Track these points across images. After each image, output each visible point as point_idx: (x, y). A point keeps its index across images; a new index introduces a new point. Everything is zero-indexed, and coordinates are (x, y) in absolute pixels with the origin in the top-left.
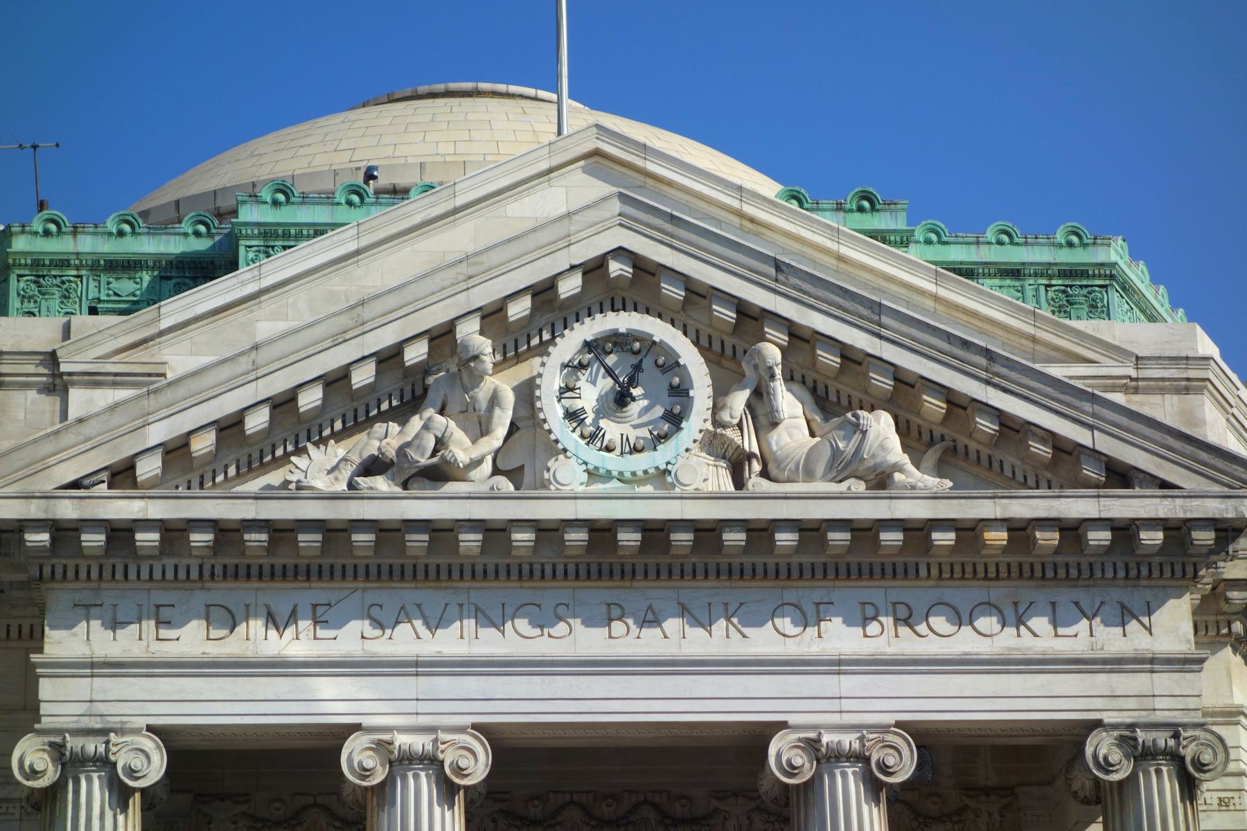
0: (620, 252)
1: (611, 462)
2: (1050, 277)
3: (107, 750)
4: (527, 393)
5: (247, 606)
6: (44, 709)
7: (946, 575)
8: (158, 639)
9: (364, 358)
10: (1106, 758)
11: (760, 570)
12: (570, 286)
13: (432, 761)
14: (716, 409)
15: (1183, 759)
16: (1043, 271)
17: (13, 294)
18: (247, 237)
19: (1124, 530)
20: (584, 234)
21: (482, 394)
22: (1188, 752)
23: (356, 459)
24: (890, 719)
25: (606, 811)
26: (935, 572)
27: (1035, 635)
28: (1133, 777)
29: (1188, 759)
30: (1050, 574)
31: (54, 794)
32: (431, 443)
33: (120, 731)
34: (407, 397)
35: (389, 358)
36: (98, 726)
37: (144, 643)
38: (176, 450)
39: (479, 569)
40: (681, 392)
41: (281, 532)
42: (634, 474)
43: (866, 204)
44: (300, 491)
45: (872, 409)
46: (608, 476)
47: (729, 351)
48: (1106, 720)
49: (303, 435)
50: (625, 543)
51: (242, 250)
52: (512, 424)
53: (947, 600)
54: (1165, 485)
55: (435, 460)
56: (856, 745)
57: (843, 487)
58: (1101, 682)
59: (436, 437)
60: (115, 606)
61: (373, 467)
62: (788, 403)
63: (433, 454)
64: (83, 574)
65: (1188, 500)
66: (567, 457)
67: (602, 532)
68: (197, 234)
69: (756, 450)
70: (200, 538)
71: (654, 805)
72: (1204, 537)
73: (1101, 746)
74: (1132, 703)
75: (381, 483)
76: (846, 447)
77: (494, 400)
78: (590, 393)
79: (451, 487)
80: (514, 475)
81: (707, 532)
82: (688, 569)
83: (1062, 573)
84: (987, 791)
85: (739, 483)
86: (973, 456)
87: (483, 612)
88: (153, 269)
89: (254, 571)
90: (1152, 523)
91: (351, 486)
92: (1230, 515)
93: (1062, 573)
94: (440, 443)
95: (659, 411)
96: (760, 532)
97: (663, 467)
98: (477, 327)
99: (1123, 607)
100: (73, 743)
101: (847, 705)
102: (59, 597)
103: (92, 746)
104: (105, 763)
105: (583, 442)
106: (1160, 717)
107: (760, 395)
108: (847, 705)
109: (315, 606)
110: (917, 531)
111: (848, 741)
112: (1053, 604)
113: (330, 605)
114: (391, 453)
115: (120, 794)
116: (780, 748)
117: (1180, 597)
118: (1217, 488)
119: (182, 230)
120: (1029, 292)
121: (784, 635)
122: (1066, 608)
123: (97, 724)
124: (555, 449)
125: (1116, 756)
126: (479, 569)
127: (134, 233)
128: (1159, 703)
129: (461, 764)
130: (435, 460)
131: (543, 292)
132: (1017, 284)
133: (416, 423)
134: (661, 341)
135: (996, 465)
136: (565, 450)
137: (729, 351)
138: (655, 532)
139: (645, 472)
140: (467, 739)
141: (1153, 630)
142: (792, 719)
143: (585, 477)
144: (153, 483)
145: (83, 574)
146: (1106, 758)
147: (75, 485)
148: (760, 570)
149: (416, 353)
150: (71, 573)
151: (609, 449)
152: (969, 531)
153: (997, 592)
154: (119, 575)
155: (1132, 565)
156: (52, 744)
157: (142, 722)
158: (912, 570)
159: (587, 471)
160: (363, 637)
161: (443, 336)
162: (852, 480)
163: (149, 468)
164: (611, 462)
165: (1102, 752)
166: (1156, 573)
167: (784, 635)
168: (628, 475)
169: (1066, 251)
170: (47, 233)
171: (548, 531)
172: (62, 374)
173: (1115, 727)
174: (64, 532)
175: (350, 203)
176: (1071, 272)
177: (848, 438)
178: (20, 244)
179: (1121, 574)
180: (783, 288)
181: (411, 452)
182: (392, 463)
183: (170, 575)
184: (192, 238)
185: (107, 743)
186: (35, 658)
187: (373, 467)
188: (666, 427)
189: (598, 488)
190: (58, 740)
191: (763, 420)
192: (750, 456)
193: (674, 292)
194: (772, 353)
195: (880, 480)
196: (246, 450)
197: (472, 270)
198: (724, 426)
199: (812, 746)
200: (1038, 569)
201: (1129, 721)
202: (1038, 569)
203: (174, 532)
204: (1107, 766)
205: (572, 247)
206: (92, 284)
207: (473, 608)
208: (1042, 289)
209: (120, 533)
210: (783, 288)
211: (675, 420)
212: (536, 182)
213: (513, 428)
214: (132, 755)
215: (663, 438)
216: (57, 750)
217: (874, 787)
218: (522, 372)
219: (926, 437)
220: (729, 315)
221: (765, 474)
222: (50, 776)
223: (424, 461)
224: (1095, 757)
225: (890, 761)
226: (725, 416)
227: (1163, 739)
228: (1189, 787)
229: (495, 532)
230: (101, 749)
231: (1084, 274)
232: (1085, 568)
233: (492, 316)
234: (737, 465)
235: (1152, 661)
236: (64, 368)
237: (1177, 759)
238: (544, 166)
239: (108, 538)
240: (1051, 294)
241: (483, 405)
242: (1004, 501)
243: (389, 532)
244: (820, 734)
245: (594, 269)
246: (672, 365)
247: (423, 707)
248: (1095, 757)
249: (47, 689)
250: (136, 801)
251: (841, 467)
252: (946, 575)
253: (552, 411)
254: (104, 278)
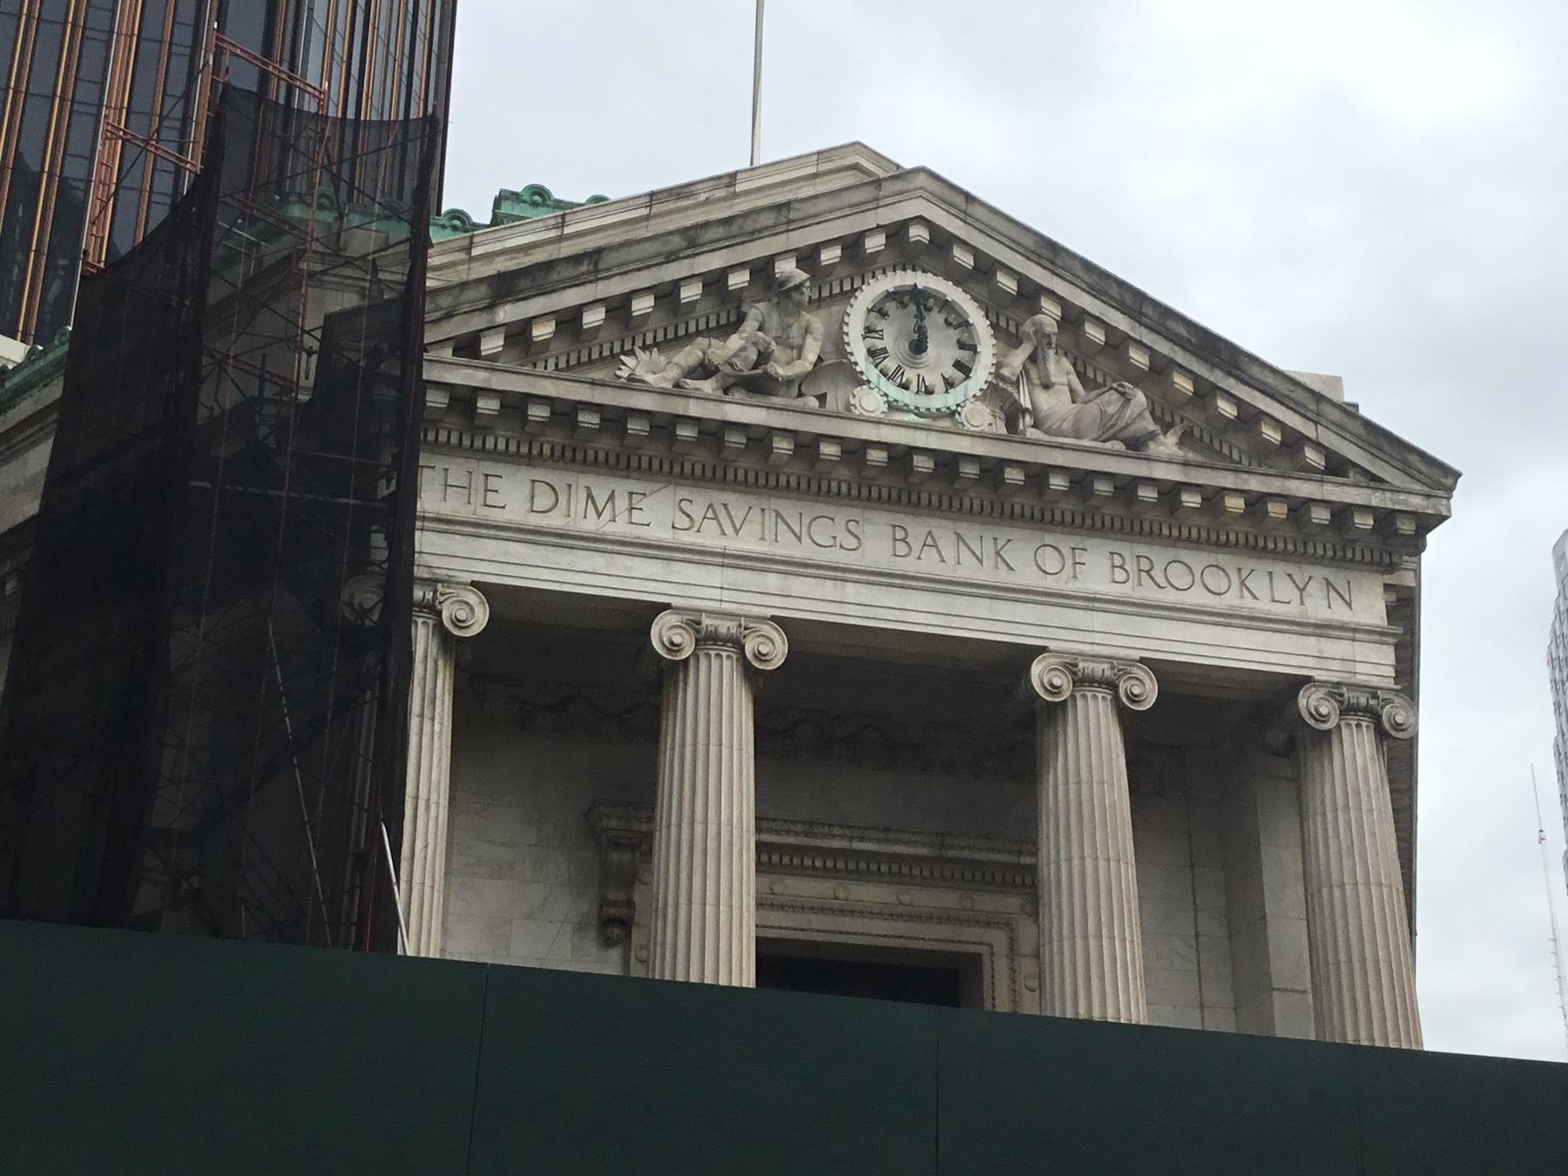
0: (921, 220)
1: (906, 397)
3: (435, 598)
8: (486, 505)
9: (693, 276)
10: (1316, 709)
14: (998, 366)
19: (1342, 513)
20: (890, 200)
24: (1137, 655)
27: (1255, 597)
29: (1384, 718)
32: (754, 356)
33: (447, 582)
35: (715, 282)
36: (426, 576)
37: (472, 507)
38: (518, 334)
42: (928, 409)
44: (633, 383)
46: (905, 409)
48: (1317, 678)
50: (920, 469)
53: (1182, 559)
54: (1375, 478)
55: (759, 371)
56: (1108, 673)
57: (1108, 445)
58: (1311, 644)
59: (759, 351)
60: (446, 470)
62: (1059, 369)
63: (755, 366)
65: (1396, 494)
66: (870, 388)
67: (901, 456)
69: (1029, 406)
73: (1309, 701)
74: (1336, 665)
75: (707, 386)
78: (892, 337)
87: (782, 518)
90: (1365, 509)
91: (677, 385)
92: (1430, 512)
97: (954, 408)
98: (794, 265)
99: (1328, 583)
101: (1098, 638)
105: (883, 379)
106: (1360, 679)
108: (1098, 638)
110: (1170, 492)
112: (1270, 573)
113: (644, 494)
116: (1038, 671)
118: (1418, 487)
119: (441, 222)
121: (1045, 572)
124: (858, 380)
128: (1360, 668)
129: (763, 651)
130: (759, 371)
131: (852, 245)
133: (735, 342)
134: (953, 301)
136: (869, 382)
139: (938, 410)
140: (767, 629)
141: (1353, 605)
142: (1052, 645)
143: (885, 408)
144: (493, 358)
146: (1316, 709)
151: (905, 387)
152: (1213, 497)
157: (468, 578)
159: (888, 402)
160: (674, 527)
162: (1114, 442)
163: (492, 344)
164: (906, 397)
165: (1313, 703)
167: (1045, 572)
168: (923, 410)
172: (380, 281)
173: (1323, 683)
184: (449, 231)
185: (435, 592)
187: (704, 370)
195: (1136, 445)
199: (1071, 668)
201: (1336, 680)
205: (879, 210)
207: (773, 514)
212: (802, 184)
214: (457, 606)
215: (949, 384)
230: (429, 596)
234: (1013, 416)
235: (1354, 630)
236: (381, 276)
237: (1377, 719)
238: (813, 170)
242: (1245, 476)
243: (713, 432)
244: (1076, 659)
245: (896, 232)
247: (726, 595)
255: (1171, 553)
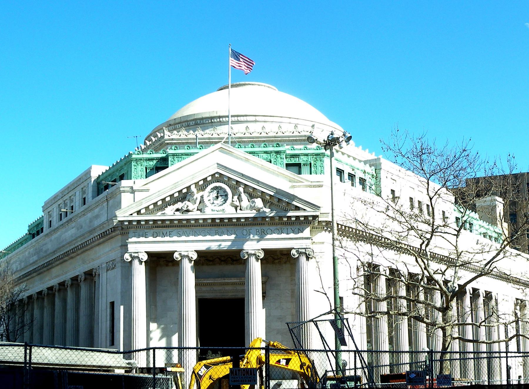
0: (217, 173)
2: (313, 156)
4: (202, 197)
5: (159, 232)
6: (129, 249)
7: (270, 224)
11: (238, 225)
12: (209, 179)
13: (188, 256)
15: (307, 254)
16: (312, 155)
17: (133, 165)
18: (170, 156)
19: (297, 217)
21: (195, 197)
22: (307, 253)
23: (175, 209)
24: (260, 248)
25: (223, 259)
26: (268, 224)
28: (299, 256)
30: (286, 224)
31: (131, 262)
33: (140, 252)
34: (184, 197)
35: (180, 192)
38: (147, 208)
39: (195, 225)
40: (226, 195)
41: (163, 221)
43: (278, 145)
45: (257, 198)
47: (236, 188)
49: (167, 205)
51: (169, 158)
52: (200, 201)
54: (305, 210)
61: (178, 210)
62: (244, 197)
64: (134, 228)
67: (213, 220)
68: (163, 153)
70: (151, 223)
71: (230, 258)
72: (311, 218)
76: (253, 205)
77: (196, 199)
79: (190, 213)
80: (200, 210)
81: (230, 219)
82: (228, 225)
83: (288, 224)
84: (285, 255)
85: (236, 211)
86: (275, 204)
88: (156, 160)
89: (160, 226)
90: (302, 216)
93: (288, 224)
94: (187, 206)
95: (223, 200)
96: (238, 219)
100: (133, 254)
102: (131, 231)
103: (136, 255)
104: (138, 257)
107: (240, 195)
109: (170, 232)
111: (253, 252)
112: (287, 229)
114: (180, 208)
115: (141, 262)
117: (308, 227)
120: (309, 158)
122: (290, 230)
123: (136, 251)
124: (206, 206)
125: (296, 253)
126: (195, 225)
127: (153, 153)
131: (205, 180)
132: (307, 157)
133: (184, 203)
135: (279, 206)
137: (236, 188)
138: (222, 219)
145: (134, 228)
147: (132, 214)
148: (238, 225)
149: (185, 191)
150: (132, 228)
153: (279, 227)
154: (139, 228)
155: (300, 222)
156: (130, 255)
158: (264, 224)
161: (189, 188)
163: (143, 211)
164: (215, 208)
166: (304, 223)
169: (317, 150)
170: (138, 154)
171: (205, 220)
174: (130, 222)
175: (187, 149)
176: (317, 155)
177: (252, 204)
178: (134, 156)
179: (298, 224)
180: (243, 178)
181: (183, 208)
182: (180, 210)
183: (147, 227)
186: (127, 241)
187: (178, 210)
188: (224, 202)
189: (213, 213)
190: (131, 254)
191: (240, 200)
192: (238, 206)
193: (226, 179)
194: (241, 189)
196: (159, 207)
197: (193, 177)
198: (233, 201)
200: (285, 223)
202: (285, 223)
203: (147, 221)
204: (294, 255)
206: (146, 163)
208: (312, 158)
209: (139, 222)
210: (243, 178)
211: (225, 201)
213: (200, 202)
216: (131, 255)
217: (257, 259)
218: (201, 193)
219: (268, 201)
220: (235, 183)
221: (241, 209)
222: (130, 259)
223: (185, 209)
224: (293, 254)
225: (259, 255)
226: (234, 200)
227: (303, 251)
228: (308, 258)
229: (196, 220)
231: (319, 155)
232: (292, 223)
233: (196, 184)
236: (134, 189)
239: (137, 223)
240: (313, 159)
241: (195, 199)
243: (180, 220)
245: (213, 175)
246: (225, 191)
248: (293, 254)
249: (129, 246)
250: (143, 263)
251: (252, 208)
252: (270, 224)
253: (206, 199)
254: (148, 162)
255: (268, 227)
